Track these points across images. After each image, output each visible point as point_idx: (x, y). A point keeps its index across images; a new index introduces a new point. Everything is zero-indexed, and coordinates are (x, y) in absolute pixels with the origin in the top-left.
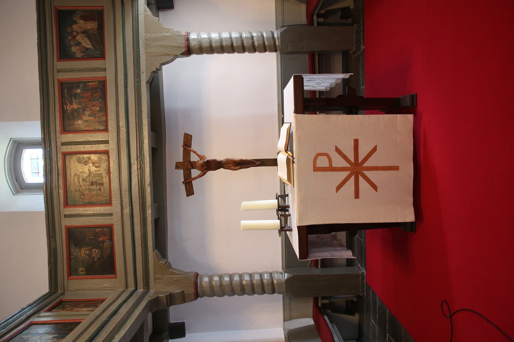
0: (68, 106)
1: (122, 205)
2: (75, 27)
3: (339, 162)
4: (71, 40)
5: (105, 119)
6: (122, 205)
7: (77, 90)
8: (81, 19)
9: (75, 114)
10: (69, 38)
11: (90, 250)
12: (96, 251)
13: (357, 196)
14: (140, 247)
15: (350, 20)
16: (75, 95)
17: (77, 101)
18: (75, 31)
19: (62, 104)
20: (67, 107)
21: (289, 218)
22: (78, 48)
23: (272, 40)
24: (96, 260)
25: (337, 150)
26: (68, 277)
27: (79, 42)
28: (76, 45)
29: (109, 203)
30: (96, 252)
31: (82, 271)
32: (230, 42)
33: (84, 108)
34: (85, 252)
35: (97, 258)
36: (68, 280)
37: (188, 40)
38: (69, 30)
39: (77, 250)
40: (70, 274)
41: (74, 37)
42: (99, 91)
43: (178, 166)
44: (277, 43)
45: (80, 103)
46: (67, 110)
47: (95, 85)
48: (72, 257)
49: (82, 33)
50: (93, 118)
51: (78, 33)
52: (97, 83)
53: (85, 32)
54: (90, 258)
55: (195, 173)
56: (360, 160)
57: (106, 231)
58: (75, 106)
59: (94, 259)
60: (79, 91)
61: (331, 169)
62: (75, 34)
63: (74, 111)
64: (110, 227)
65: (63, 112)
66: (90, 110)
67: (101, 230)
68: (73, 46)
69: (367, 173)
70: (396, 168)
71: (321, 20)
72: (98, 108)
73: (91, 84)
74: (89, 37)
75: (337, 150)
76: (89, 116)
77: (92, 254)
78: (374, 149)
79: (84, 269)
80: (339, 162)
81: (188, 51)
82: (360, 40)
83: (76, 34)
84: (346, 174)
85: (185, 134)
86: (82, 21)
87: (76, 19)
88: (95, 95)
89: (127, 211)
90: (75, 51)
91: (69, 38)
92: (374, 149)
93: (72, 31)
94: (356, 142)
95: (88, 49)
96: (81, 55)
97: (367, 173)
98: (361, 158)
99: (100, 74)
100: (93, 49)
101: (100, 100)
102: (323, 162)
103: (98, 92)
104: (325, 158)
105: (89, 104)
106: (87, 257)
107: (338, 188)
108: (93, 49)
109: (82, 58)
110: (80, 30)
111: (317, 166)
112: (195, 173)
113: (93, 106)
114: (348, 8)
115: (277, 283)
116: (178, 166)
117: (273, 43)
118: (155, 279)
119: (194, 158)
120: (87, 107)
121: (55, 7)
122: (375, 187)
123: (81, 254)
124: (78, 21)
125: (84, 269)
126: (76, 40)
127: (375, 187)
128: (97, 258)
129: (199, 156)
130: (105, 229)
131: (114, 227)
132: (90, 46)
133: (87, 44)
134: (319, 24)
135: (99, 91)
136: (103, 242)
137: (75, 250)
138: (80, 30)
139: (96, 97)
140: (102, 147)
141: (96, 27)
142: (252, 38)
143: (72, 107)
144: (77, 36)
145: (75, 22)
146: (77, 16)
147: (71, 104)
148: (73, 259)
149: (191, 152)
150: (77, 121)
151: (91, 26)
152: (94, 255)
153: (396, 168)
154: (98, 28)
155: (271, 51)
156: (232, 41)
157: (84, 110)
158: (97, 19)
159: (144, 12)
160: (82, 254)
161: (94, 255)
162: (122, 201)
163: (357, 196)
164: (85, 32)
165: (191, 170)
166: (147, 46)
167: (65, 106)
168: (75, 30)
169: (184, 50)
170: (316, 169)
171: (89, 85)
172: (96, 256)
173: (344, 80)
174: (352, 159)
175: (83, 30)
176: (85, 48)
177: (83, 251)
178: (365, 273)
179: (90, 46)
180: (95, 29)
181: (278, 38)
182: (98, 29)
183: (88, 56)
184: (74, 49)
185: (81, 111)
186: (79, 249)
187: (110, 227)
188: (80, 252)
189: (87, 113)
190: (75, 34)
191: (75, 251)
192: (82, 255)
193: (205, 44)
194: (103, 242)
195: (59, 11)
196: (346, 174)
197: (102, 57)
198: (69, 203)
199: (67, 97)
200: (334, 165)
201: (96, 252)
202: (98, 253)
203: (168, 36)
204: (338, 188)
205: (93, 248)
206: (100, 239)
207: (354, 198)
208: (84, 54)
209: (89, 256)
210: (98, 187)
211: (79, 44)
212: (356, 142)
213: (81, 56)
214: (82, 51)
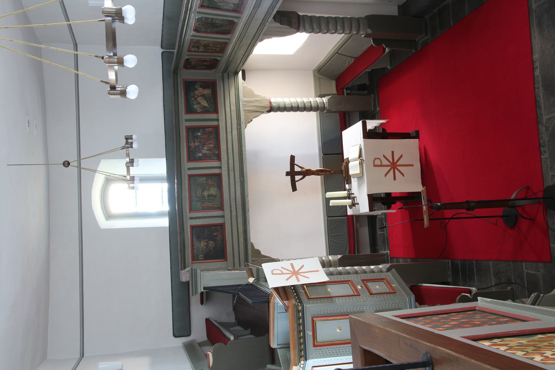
0: (192, 144)
1: (231, 210)
2: (196, 92)
3: (385, 162)
4: (194, 100)
5: (218, 153)
6: (231, 210)
7: (198, 133)
8: (201, 87)
9: (197, 149)
10: (193, 99)
11: (207, 242)
12: (211, 243)
13: (395, 179)
14: (242, 238)
15: (366, 92)
16: (197, 137)
17: (198, 140)
18: (197, 95)
19: (188, 142)
20: (191, 144)
21: (355, 198)
22: (198, 106)
23: (323, 104)
24: (211, 249)
25: (384, 156)
26: (192, 261)
27: (199, 102)
28: (197, 104)
29: (221, 208)
30: (211, 244)
31: (201, 257)
32: (297, 104)
33: (203, 145)
34: (204, 245)
35: (212, 247)
36: (192, 263)
37: (270, 103)
38: (192, 94)
39: (198, 243)
40: (193, 259)
41: (196, 99)
42: (213, 134)
43: (288, 174)
44: (326, 106)
45: (200, 142)
46: (191, 146)
47: (210, 130)
48: (194, 247)
49: (201, 96)
50: (209, 152)
51: (198, 96)
52: (211, 129)
53: (203, 96)
54: (207, 248)
55: (297, 178)
56: (395, 161)
57: (219, 228)
58: (197, 144)
59: (210, 248)
60: (199, 134)
61: (382, 165)
62: (196, 97)
63: (196, 147)
64: (222, 226)
65: (188, 147)
66: (208, 146)
67: (215, 227)
68: (195, 104)
69: (399, 168)
70: (412, 165)
71: (349, 92)
72: (213, 145)
73: (208, 129)
74: (206, 99)
75: (384, 156)
76: (207, 150)
77: (208, 244)
78: (401, 156)
79: (203, 256)
80: (385, 162)
81: (272, 109)
82: (376, 104)
83: (197, 97)
84: (389, 168)
85: (291, 155)
86: (201, 88)
87: (197, 87)
88: (210, 137)
89: (234, 213)
90: (196, 108)
91: (193, 99)
92: (401, 156)
93: (195, 95)
94: (393, 152)
95: (205, 106)
96: (201, 110)
97: (399, 168)
98: (395, 160)
99: (215, 123)
100: (209, 107)
101: (214, 140)
102: (378, 162)
103: (213, 135)
104: (379, 160)
105: (206, 143)
106: (205, 247)
107: (386, 175)
108: (209, 107)
109: (202, 113)
110: (200, 95)
111: (376, 164)
112: (297, 178)
113: (209, 144)
114: (365, 84)
115: (333, 261)
116: (288, 174)
117: (323, 105)
118: (253, 261)
119: (297, 169)
120: (205, 144)
121: (184, 79)
122: (403, 175)
123: (201, 245)
124: (198, 89)
125: (203, 256)
126: (197, 101)
127: (403, 175)
128: (212, 247)
129: (300, 167)
130: (217, 227)
131: (226, 225)
132: (206, 105)
133: (205, 103)
134: (347, 94)
135: (213, 134)
136: (216, 236)
137: (196, 242)
138: (200, 95)
139: (211, 138)
140: (217, 171)
141: (210, 93)
142: (311, 102)
143: (194, 144)
144: (197, 98)
145: (197, 89)
146: (198, 85)
147: (194, 142)
148: (195, 249)
149: (295, 165)
150: (199, 153)
151: (207, 92)
152: (210, 245)
153: (412, 165)
154: (212, 93)
155: (315, 111)
156: (298, 104)
157: (203, 147)
158: (211, 87)
159: (243, 84)
160: (201, 245)
161: (210, 245)
162: (231, 207)
163: (395, 179)
164: (203, 96)
165: (295, 176)
166: (245, 106)
167: (190, 144)
168: (196, 94)
169: (268, 109)
170: (375, 166)
171: (206, 130)
172: (211, 246)
173: (382, 124)
174: (391, 160)
175: (202, 94)
176: (203, 106)
177: (202, 243)
178: (389, 252)
179: (206, 105)
180: (209, 94)
181: (326, 102)
182: (212, 94)
183: (205, 111)
184: (196, 107)
185: (201, 147)
186: (199, 242)
187: (222, 226)
188: (200, 244)
189: (205, 148)
190: (196, 97)
191: (196, 244)
192: (202, 246)
193: (282, 105)
194: (216, 236)
195: (185, 81)
196: (389, 168)
197: (216, 111)
198: (192, 210)
199: (191, 138)
200: (383, 164)
201: (211, 244)
202: (213, 244)
203: (258, 100)
204: (386, 175)
205: (209, 241)
206: (215, 234)
207: (393, 180)
208: (202, 110)
209: (207, 246)
210: (213, 198)
211: (199, 103)
212: (393, 152)
213: (201, 111)
214: (201, 108)
